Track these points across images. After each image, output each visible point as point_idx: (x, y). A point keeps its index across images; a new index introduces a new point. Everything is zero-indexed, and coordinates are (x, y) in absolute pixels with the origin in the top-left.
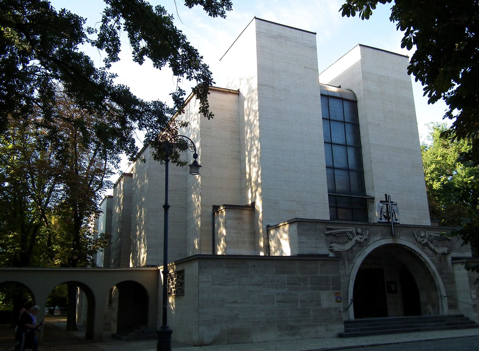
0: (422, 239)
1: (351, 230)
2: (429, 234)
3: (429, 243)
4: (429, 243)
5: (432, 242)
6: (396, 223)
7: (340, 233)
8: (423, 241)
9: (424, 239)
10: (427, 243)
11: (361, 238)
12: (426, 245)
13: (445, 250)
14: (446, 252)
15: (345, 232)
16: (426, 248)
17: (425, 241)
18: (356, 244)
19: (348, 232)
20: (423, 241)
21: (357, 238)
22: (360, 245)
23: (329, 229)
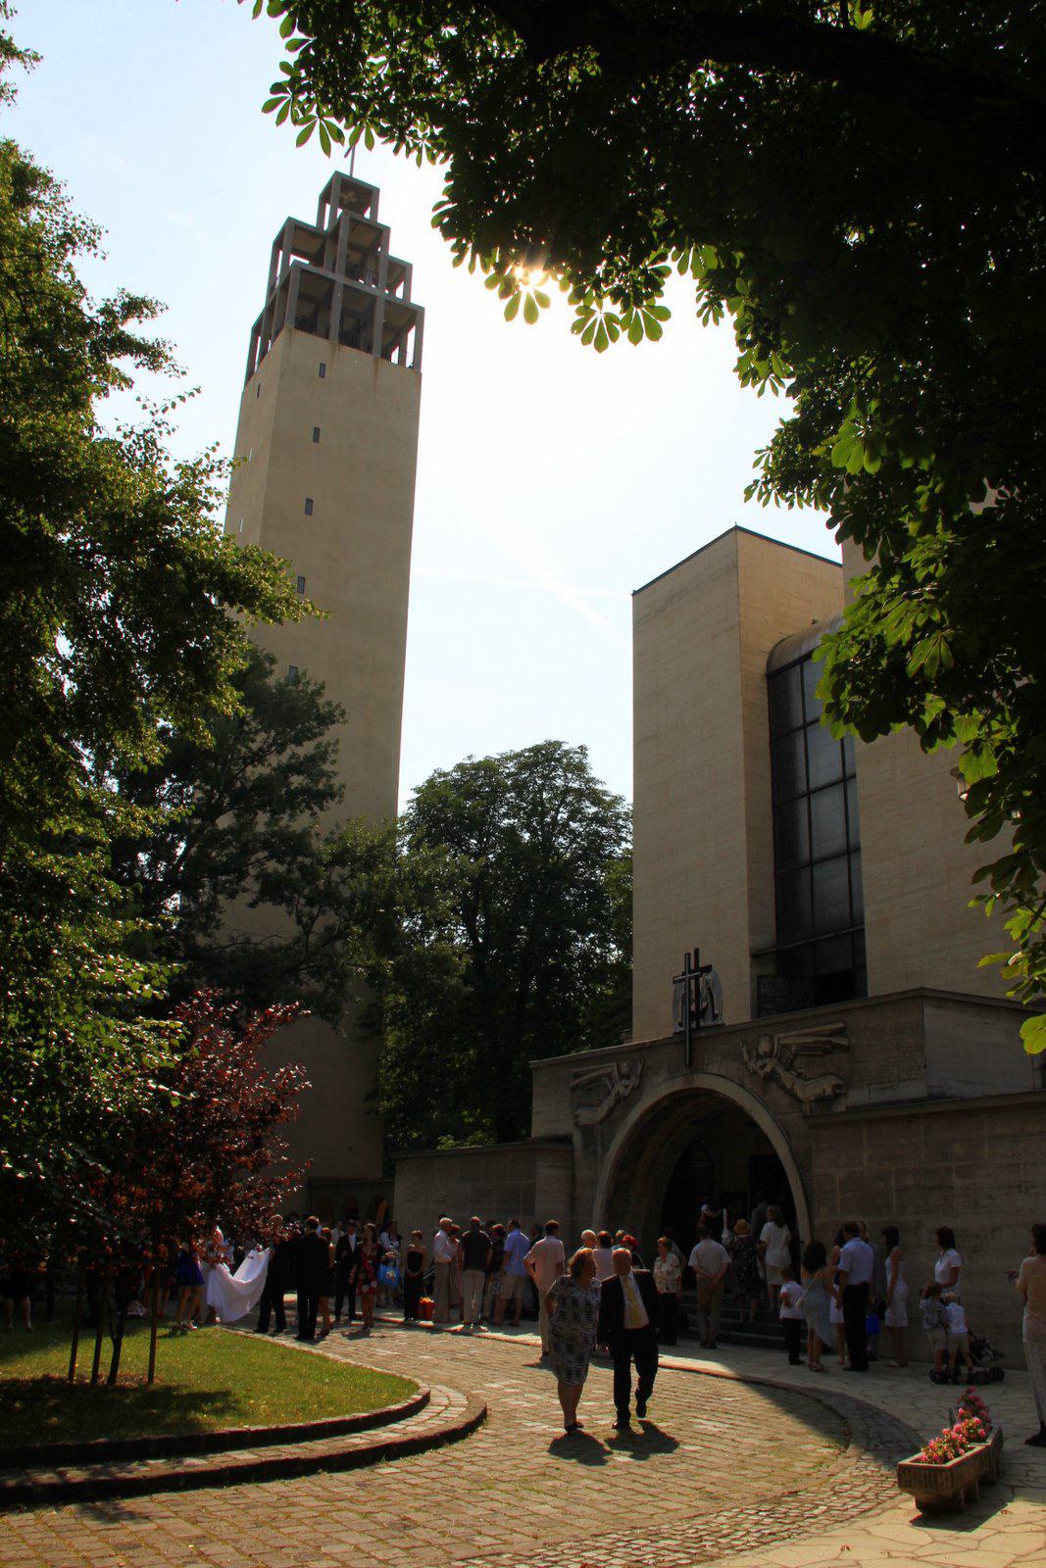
0: (760, 1063)
1: (609, 1070)
2: (782, 1042)
3: (780, 1070)
4: (780, 1070)
5: (789, 1068)
6: (716, 1026)
7: (592, 1081)
8: (763, 1067)
9: (766, 1061)
10: (773, 1070)
11: (626, 1087)
12: (772, 1077)
13: (826, 1086)
14: (829, 1091)
15: (599, 1078)
16: (774, 1086)
17: (768, 1069)
18: (617, 1102)
19: (603, 1075)
20: (763, 1067)
21: (620, 1088)
22: (625, 1103)
23: (577, 1075)
